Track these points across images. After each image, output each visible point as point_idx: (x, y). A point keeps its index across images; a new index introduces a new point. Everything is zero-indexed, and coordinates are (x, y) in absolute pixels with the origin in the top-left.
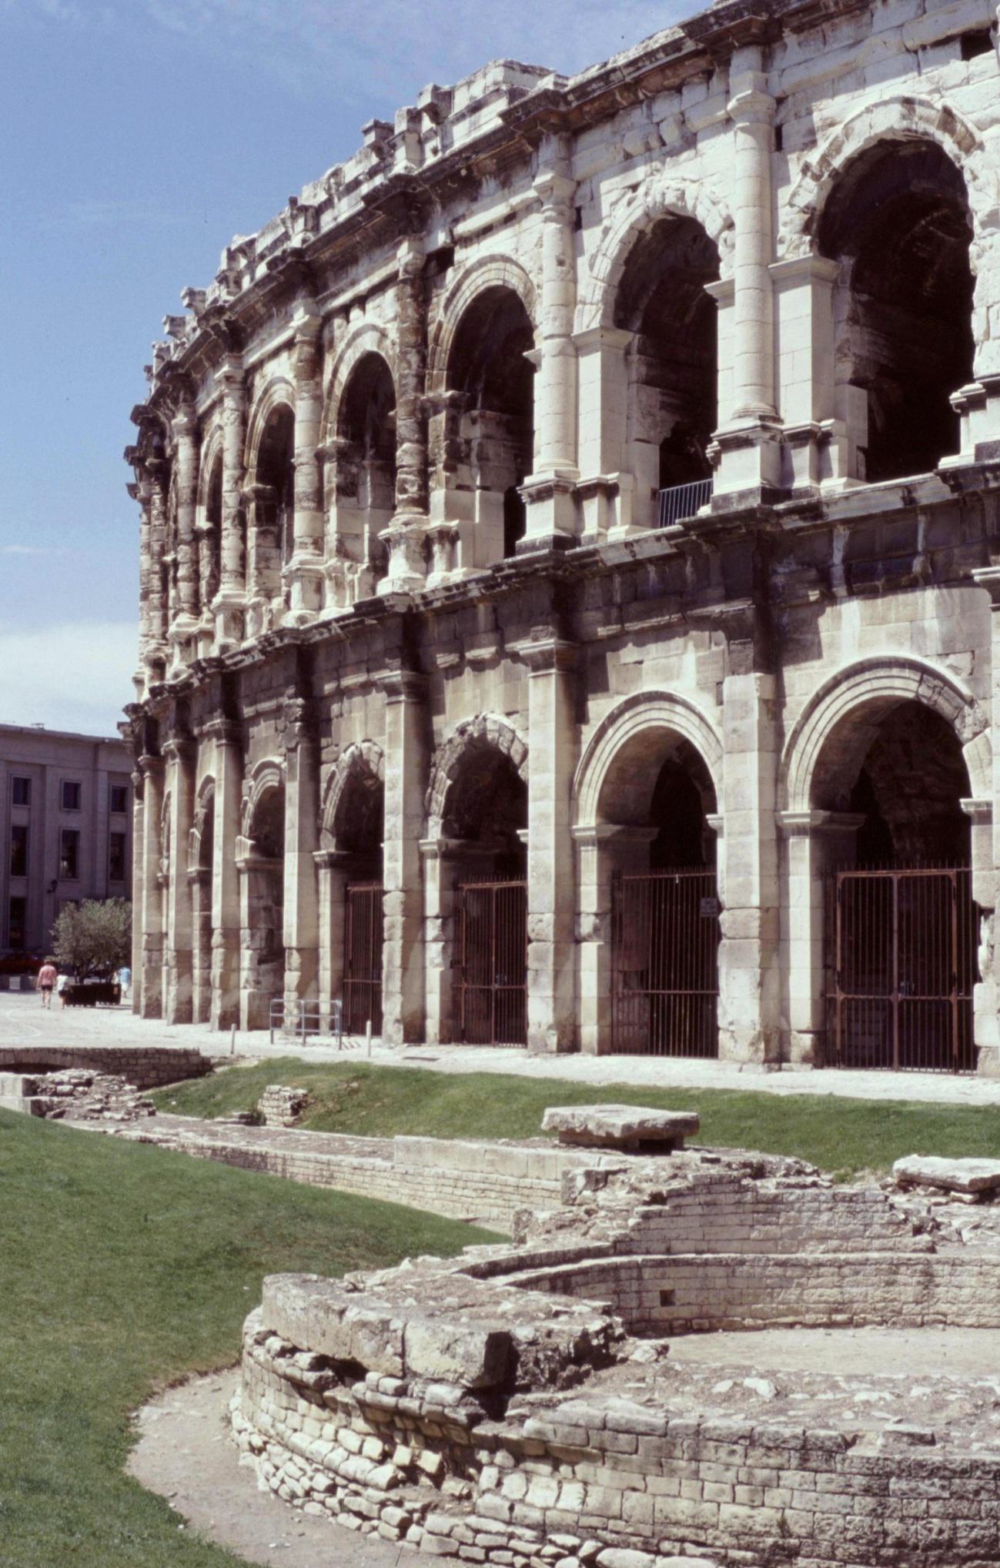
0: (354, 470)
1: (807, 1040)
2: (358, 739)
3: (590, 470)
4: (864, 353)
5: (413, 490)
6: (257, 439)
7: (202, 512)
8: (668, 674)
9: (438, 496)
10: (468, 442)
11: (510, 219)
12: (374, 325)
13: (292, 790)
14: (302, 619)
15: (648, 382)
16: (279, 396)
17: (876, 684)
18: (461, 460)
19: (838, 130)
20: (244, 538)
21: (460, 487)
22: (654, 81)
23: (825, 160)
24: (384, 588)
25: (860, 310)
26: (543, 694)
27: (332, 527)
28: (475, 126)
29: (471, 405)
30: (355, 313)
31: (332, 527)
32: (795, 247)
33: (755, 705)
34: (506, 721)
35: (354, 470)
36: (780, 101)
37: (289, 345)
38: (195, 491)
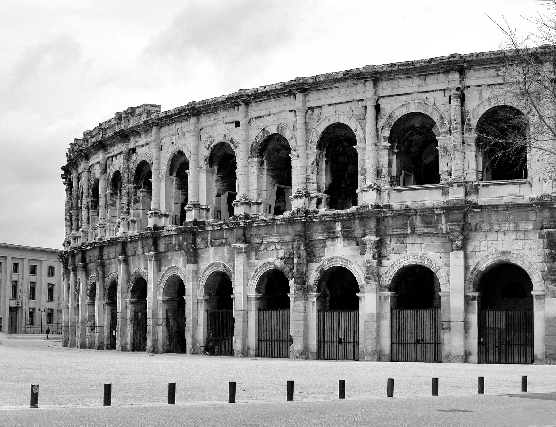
0: (115, 199)
1: (203, 349)
2: (113, 272)
3: (163, 210)
4: (220, 189)
5: (125, 209)
6: (92, 186)
7: (79, 201)
8: (177, 262)
9: (131, 211)
10: (139, 197)
11: (147, 144)
12: (118, 164)
13: (97, 284)
14: (100, 239)
15: (178, 188)
16: (97, 176)
17: (218, 268)
18: (137, 202)
19: (212, 139)
20: (88, 213)
21: (137, 209)
22: (176, 120)
23: (209, 145)
24: (118, 235)
25: (219, 178)
26: (152, 265)
27: (108, 214)
28: (140, 119)
29: (140, 188)
30: (114, 158)
31: (108, 214)
32: (204, 164)
33: (192, 271)
34: (144, 271)
35: (115, 199)
36: (201, 129)
37: (99, 162)
38: (77, 195)
